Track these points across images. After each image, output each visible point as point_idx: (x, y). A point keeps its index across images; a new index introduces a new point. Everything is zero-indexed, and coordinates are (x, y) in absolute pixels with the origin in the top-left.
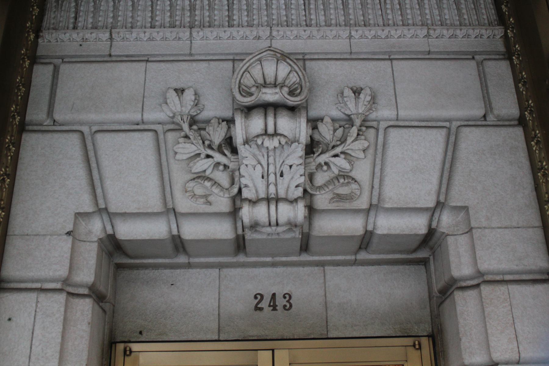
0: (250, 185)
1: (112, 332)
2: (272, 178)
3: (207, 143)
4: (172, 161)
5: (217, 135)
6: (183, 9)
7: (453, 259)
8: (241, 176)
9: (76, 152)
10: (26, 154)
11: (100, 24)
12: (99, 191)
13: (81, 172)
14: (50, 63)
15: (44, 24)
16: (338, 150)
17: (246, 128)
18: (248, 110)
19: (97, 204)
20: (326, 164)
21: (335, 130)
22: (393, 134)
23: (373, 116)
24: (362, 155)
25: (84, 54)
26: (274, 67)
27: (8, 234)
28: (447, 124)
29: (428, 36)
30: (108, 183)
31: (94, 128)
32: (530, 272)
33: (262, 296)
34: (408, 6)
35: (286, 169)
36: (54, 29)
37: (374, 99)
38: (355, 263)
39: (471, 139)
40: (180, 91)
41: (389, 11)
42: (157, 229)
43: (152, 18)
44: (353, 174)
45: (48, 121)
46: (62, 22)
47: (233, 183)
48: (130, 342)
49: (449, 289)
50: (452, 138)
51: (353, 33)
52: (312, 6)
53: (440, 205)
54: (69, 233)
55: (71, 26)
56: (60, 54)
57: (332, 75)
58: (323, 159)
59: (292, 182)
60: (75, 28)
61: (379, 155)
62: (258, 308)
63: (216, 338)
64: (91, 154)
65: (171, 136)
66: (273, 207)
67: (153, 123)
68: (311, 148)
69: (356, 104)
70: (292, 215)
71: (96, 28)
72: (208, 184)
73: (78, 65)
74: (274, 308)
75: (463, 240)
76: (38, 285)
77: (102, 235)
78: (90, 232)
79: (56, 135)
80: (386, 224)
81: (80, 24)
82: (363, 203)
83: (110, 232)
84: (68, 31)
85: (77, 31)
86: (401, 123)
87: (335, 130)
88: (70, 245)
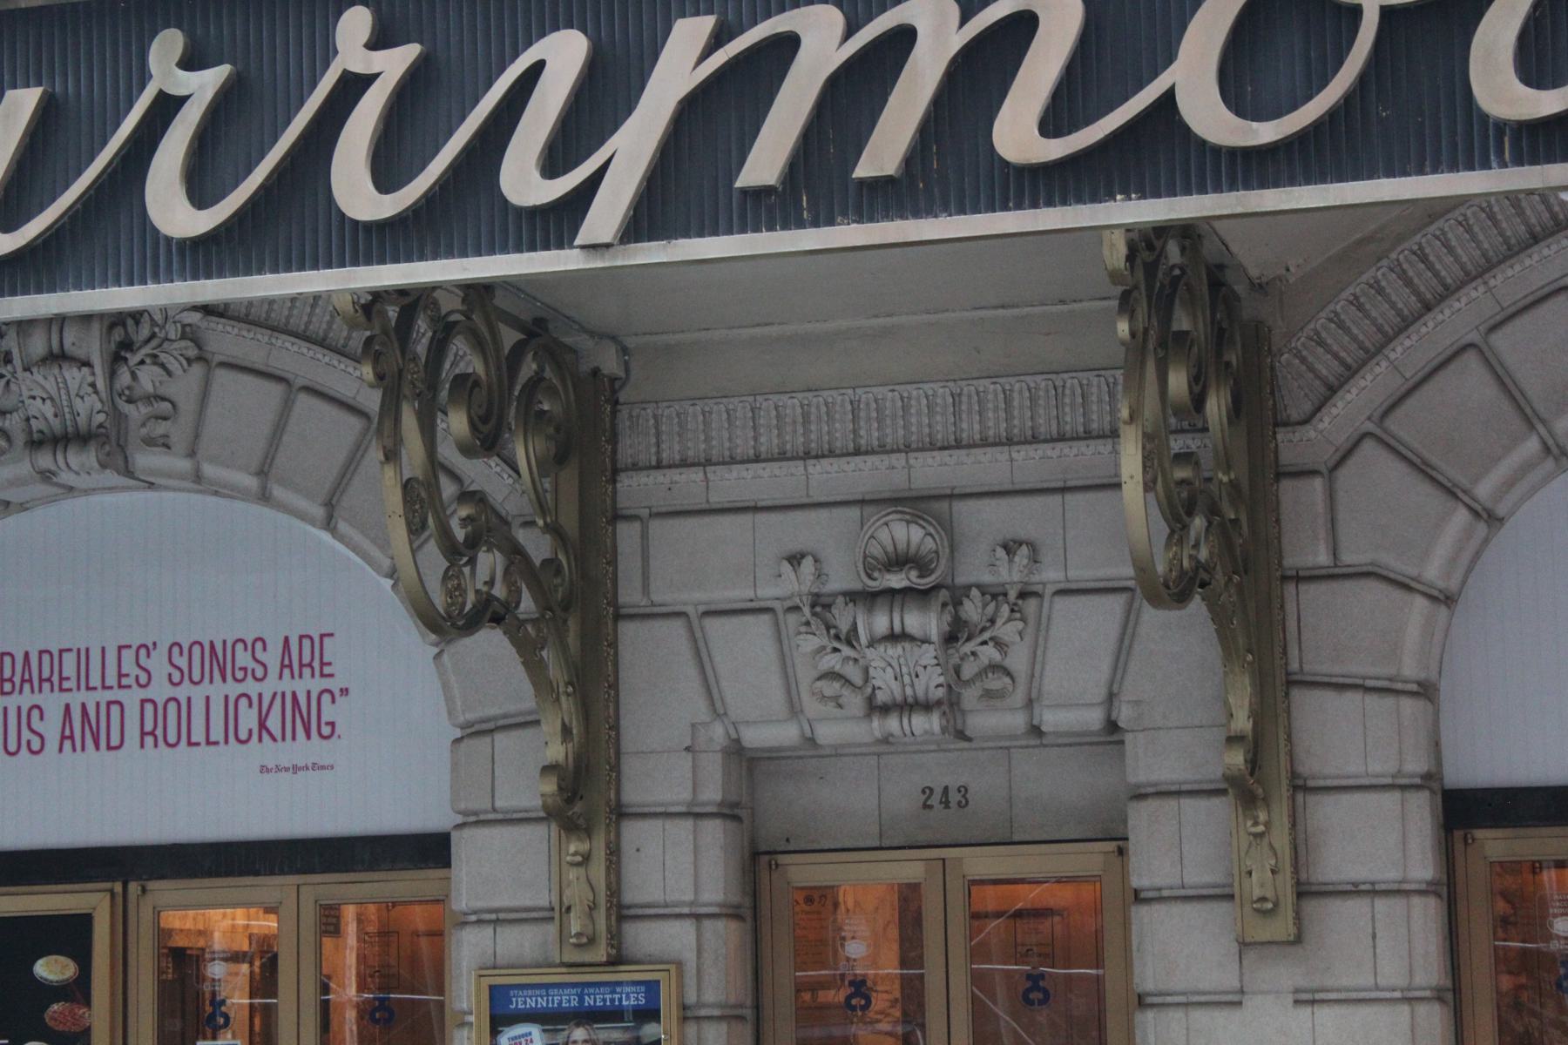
1: (753, 841)
2: (907, 679)
3: (833, 631)
6: (794, 422)
12: (715, 691)
13: (692, 671)
16: (986, 636)
19: (715, 711)
20: (974, 654)
21: (985, 606)
22: (1062, 603)
23: (1036, 578)
24: (1018, 638)
30: (724, 684)
31: (702, 609)
32: (1211, 781)
33: (931, 790)
34: (1094, 398)
35: (920, 670)
37: (1035, 559)
40: (795, 559)
41: (1067, 409)
42: (785, 734)
43: (755, 439)
44: (1007, 663)
51: (1015, 455)
52: (964, 407)
53: (1111, 697)
54: (687, 749)
57: (984, 522)
59: (930, 683)
61: (1043, 633)
62: (926, 806)
63: (877, 844)
65: (792, 619)
66: (905, 721)
68: (950, 639)
69: (1010, 570)
70: (927, 726)
72: (837, 685)
74: (947, 805)
78: (711, 739)
82: (1019, 697)
83: (734, 736)
86: (1074, 586)
87: (985, 606)
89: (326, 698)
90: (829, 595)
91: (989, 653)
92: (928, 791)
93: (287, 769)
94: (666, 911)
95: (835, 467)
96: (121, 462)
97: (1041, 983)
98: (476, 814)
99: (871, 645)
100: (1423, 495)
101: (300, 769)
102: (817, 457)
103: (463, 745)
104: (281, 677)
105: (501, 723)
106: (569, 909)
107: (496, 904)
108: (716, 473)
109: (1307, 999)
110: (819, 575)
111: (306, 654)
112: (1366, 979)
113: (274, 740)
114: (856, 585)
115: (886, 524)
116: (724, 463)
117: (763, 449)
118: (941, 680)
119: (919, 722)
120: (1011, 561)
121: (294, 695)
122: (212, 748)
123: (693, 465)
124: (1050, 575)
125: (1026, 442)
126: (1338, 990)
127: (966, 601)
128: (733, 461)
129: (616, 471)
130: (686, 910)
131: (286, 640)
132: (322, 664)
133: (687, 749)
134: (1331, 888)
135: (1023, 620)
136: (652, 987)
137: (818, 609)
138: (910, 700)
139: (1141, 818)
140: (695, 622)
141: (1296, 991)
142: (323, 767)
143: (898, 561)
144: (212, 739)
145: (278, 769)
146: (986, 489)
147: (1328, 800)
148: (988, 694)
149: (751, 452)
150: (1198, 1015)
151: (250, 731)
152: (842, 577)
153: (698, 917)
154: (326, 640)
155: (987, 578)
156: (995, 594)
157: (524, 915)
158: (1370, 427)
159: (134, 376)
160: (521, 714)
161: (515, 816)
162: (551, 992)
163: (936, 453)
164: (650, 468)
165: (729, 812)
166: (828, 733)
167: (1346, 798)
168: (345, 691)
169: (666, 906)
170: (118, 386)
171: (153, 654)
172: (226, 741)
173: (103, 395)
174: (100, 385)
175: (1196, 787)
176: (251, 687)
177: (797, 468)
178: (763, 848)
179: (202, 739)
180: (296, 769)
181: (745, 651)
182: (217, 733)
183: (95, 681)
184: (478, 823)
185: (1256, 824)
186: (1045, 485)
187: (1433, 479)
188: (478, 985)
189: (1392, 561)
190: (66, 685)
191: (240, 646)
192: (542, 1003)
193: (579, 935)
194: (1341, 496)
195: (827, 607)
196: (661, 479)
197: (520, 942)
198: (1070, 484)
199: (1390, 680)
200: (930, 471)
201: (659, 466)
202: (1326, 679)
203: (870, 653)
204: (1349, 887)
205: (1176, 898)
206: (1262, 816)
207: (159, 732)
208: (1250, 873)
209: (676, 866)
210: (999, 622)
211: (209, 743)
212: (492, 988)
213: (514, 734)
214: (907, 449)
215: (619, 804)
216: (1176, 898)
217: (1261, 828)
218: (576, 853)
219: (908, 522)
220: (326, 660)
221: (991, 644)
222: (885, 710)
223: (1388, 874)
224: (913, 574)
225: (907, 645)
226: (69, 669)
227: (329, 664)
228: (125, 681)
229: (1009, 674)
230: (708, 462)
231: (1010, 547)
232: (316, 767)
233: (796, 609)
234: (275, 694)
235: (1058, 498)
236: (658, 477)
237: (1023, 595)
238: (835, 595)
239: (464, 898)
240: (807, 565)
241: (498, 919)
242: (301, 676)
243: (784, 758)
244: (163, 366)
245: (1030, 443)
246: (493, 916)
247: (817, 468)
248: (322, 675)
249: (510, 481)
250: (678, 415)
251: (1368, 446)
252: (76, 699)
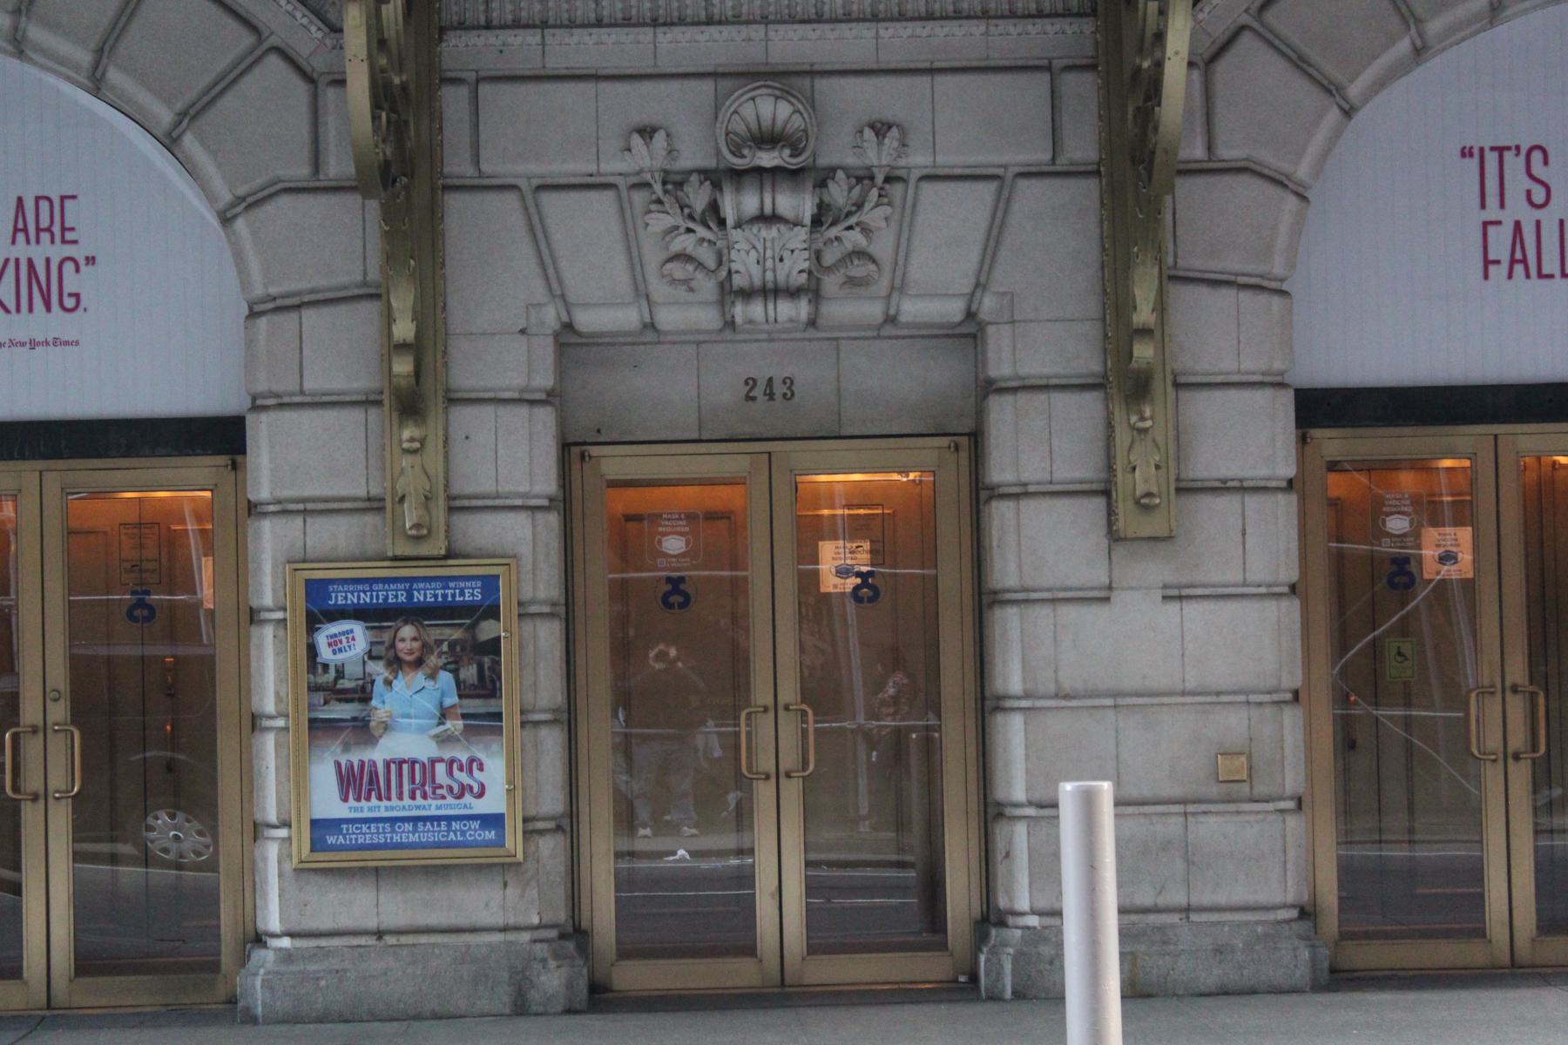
0: (742, 270)
2: (769, 263)
3: (686, 211)
4: (641, 233)
5: (698, 197)
7: (991, 355)
8: (731, 261)
9: (517, 219)
12: (551, 271)
13: (527, 250)
16: (853, 220)
17: (738, 206)
18: (737, 175)
19: (550, 290)
20: (837, 238)
21: (851, 189)
22: (928, 189)
23: (902, 162)
24: (883, 224)
26: (771, 107)
28: (1000, 172)
29: (987, 34)
30: (563, 264)
31: (536, 182)
32: (1081, 376)
33: (755, 381)
35: (786, 254)
38: (878, 337)
39: (1031, 194)
40: (647, 132)
42: (628, 318)
44: (872, 249)
47: (720, 263)
48: (585, 443)
49: (988, 388)
50: (1005, 193)
53: (980, 286)
54: (523, 332)
58: (834, 232)
59: (794, 268)
62: (750, 398)
63: (695, 436)
64: (535, 219)
65: (639, 197)
66: (771, 306)
67: (612, 174)
68: (817, 222)
69: (879, 152)
70: (793, 313)
72: (690, 268)
74: (771, 396)
75: (1006, 330)
76: (491, 395)
77: (557, 327)
78: (543, 323)
80: (912, 309)
82: (882, 287)
86: (940, 172)
87: (851, 189)
88: (525, 347)
89: (69, 267)
90: (678, 173)
91: (855, 238)
92: (751, 382)
93: (23, 344)
94: (497, 502)
95: (688, 36)
97: (682, 587)
98: (278, 396)
99: (738, 225)
100: (1301, 89)
101: (38, 344)
102: (665, 24)
103: (263, 322)
104: (14, 242)
105: (306, 299)
106: (403, 498)
107: (307, 493)
108: (555, 37)
109: (1176, 595)
110: (671, 152)
111: (41, 217)
112: (1234, 575)
113: (7, 311)
114: (710, 163)
115: (753, 99)
116: (561, 26)
117: (605, 13)
118: (806, 265)
119: (786, 309)
120: (880, 144)
121: (30, 263)
123: (527, 26)
124: (919, 160)
125: (892, 20)
126: (1204, 586)
127: (831, 184)
128: (572, 25)
129: (442, 31)
130: (518, 502)
131: (20, 200)
132: (64, 229)
133: (523, 332)
134: (1199, 484)
135: (889, 204)
136: (490, 583)
137: (670, 187)
138: (770, 285)
139: (1001, 412)
140: (529, 198)
141: (1165, 587)
142: (67, 343)
143: (768, 139)
145: (12, 343)
146: (848, 67)
147: (1202, 396)
148: (851, 282)
149: (592, 16)
150: (1069, 613)
152: (693, 155)
153: (534, 509)
154: (68, 203)
155: (851, 160)
156: (864, 177)
157: (335, 506)
158: (1245, 19)
160: (330, 289)
161: (325, 399)
162: (375, 587)
163: (796, 26)
164: (478, 27)
165: (551, 398)
166: (668, 318)
167: (1218, 394)
168: (91, 260)
169: (498, 497)
175: (1064, 381)
177: (646, 35)
178: (571, 439)
180: (34, 344)
181: (588, 232)
184: (281, 406)
185: (1142, 419)
186: (912, 66)
187: (1310, 76)
188: (293, 577)
189: (1269, 158)
192: (365, 599)
193: (417, 526)
194: (1219, 87)
195: (679, 185)
196: (492, 40)
197: (335, 535)
198: (937, 65)
199: (1261, 277)
200: (790, 45)
201: (488, 26)
202: (1198, 275)
203: (736, 235)
204: (1217, 484)
205: (1044, 494)
206: (1148, 413)
208: (1134, 469)
209: (508, 455)
210: (867, 206)
212: (308, 582)
213: (327, 312)
214: (765, 20)
215: (448, 390)
216: (1044, 494)
217: (1148, 424)
218: (412, 440)
219: (777, 98)
220: (67, 225)
221: (858, 229)
222: (747, 294)
223: (1257, 471)
224: (787, 152)
225: (782, 227)
227: (72, 229)
229: (874, 261)
230: (544, 25)
231: (881, 129)
232: (56, 342)
233: (647, 185)
234: (7, 261)
235: (925, 81)
236: (490, 38)
237: (888, 180)
238: (690, 172)
239: (262, 487)
240: (660, 139)
241: (308, 509)
242: (38, 242)
243: (599, 344)
245: (898, 20)
246: (301, 506)
247: (666, 37)
248: (64, 241)
249: (320, 35)
251: (1246, 39)
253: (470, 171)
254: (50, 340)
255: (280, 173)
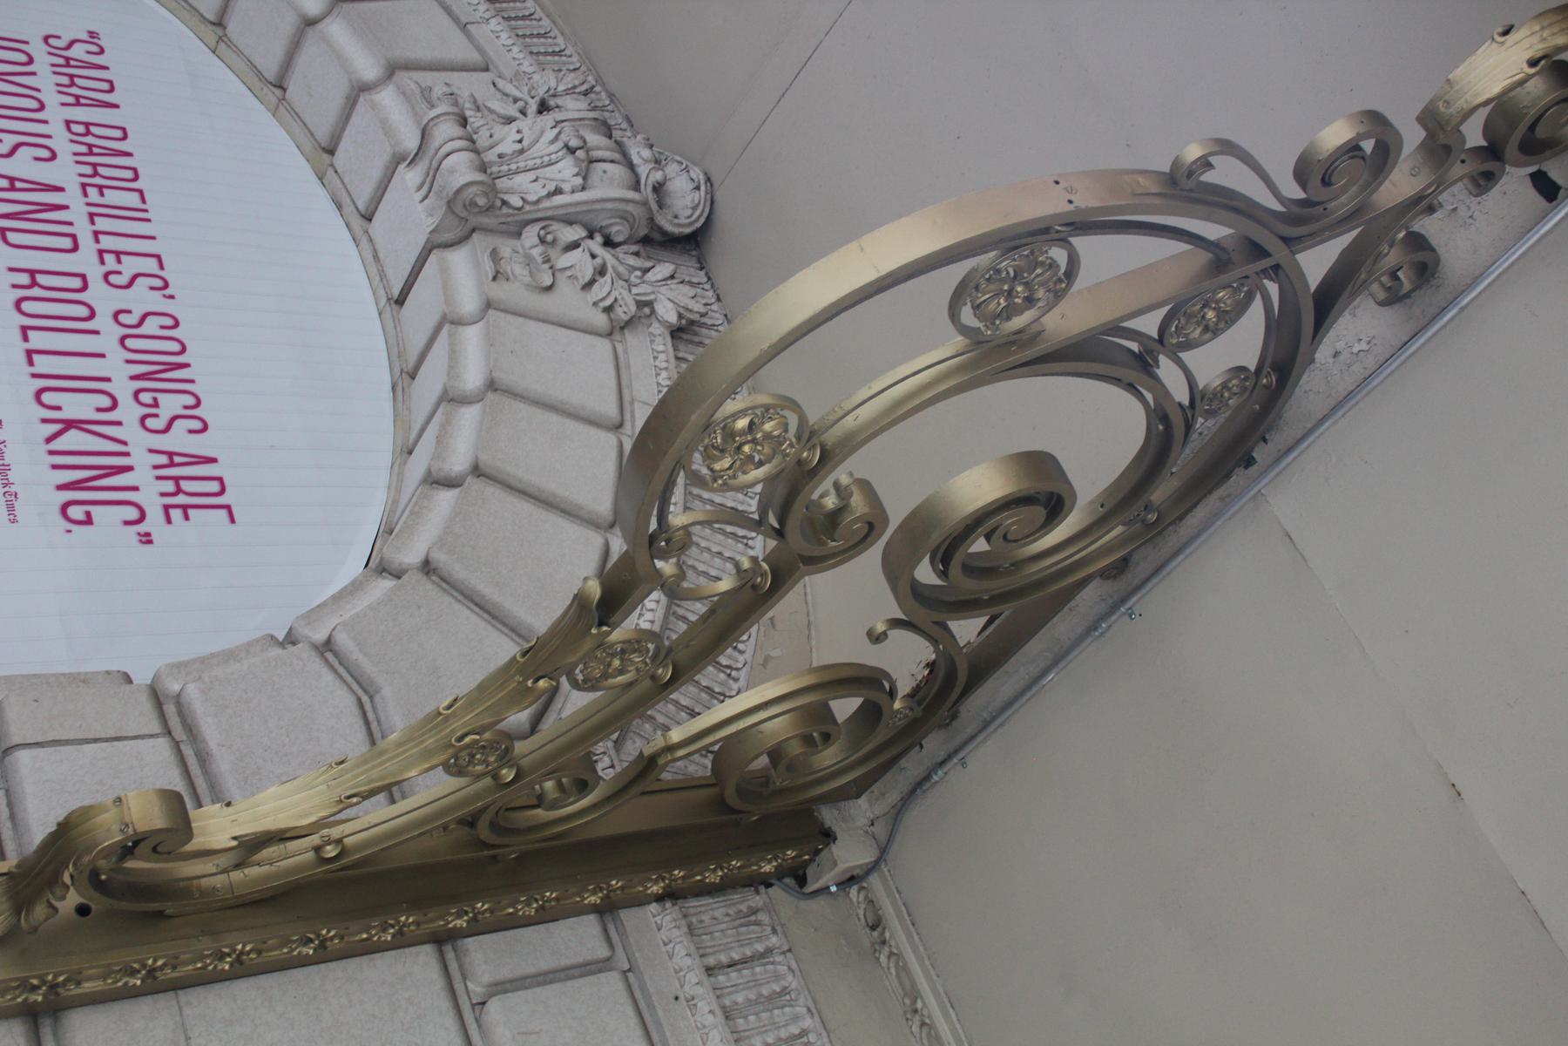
10: (383, 964)
11: (741, 1021)
14: (611, 946)
15: (693, 903)
25: (660, 1013)
27: (180, 992)
36: (689, 926)
45: (478, 989)
46: (713, 939)
55: (711, 961)
56: (640, 961)
60: (710, 971)
71: (727, 1018)
73: (630, 1010)
79: (450, 1021)
81: (721, 978)
84: (698, 959)
85: (704, 978)
96: (446, 237)
111: (193, 487)
113: (49, 440)
122: (23, 358)
131: (213, 460)
132: (185, 508)
142: (11, 508)
144: (36, 357)
151: (59, 408)
154: (224, 512)
159: (574, 246)
168: (146, 539)
170: (555, 226)
171: (158, 294)
172: (34, 376)
173: (546, 204)
174: (558, 200)
176: (129, 412)
179: (32, 345)
182: (43, 364)
183: (102, 224)
190: (92, 192)
191: (190, 401)
207: (36, 292)
211: (30, 353)
220: (191, 512)
226: (112, 197)
227: (187, 518)
228: (109, 258)
234: (125, 443)
244: (592, 282)
250: (785, 991)
252: (72, 196)
253: (477, 989)
254: (13, 489)
255: (387, 692)
